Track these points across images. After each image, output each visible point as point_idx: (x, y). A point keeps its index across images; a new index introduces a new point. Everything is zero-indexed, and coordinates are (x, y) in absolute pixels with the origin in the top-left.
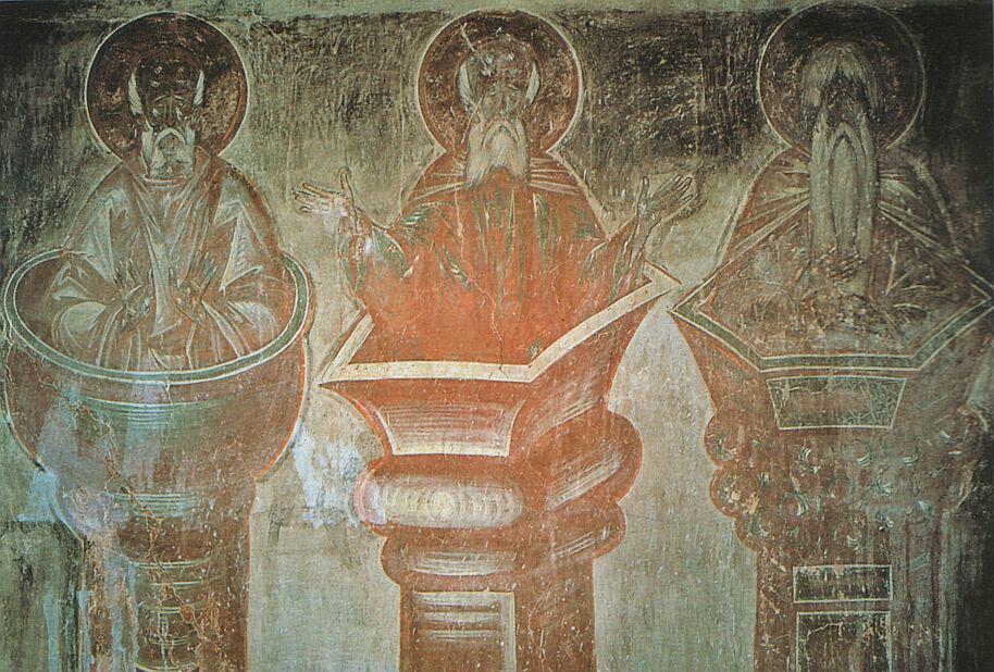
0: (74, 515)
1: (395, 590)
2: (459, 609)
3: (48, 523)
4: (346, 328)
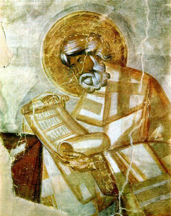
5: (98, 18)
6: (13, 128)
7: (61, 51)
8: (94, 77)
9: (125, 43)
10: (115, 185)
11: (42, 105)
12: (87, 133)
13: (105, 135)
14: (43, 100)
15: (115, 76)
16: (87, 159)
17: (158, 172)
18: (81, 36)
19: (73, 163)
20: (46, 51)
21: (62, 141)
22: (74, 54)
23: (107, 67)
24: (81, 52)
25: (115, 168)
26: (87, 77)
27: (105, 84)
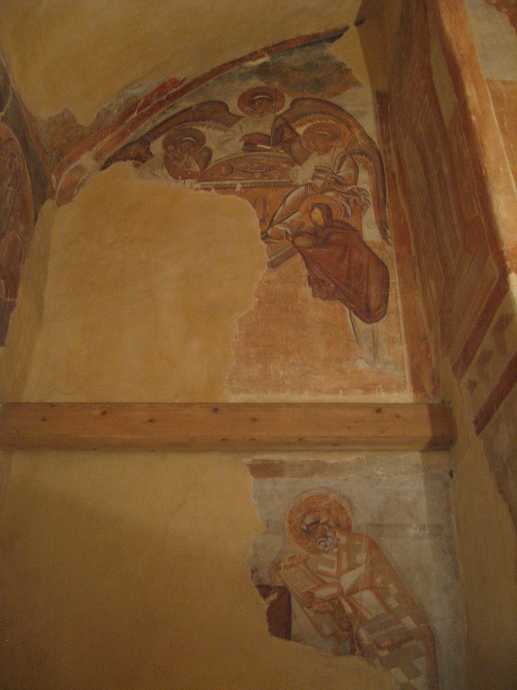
5: (328, 498)
6: (267, 581)
7: (302, 522)
8: (328, 540)
9: (350, 514)
10: (350, 623)
11: (289, 563)
12: (325, 583)
13: (339, 585)
14: (290, 559)
15: (343, 539)
16: (326, 604)
17: (382, 611)
18: (316, 511)
19: (315, 607)
20: (290, 522)
21: (306, 590)
22: (312, 524)
23: (337, 533)
24: (316, 523)
25: (349, 610)
26: (322, 541)
27: (337, 546)
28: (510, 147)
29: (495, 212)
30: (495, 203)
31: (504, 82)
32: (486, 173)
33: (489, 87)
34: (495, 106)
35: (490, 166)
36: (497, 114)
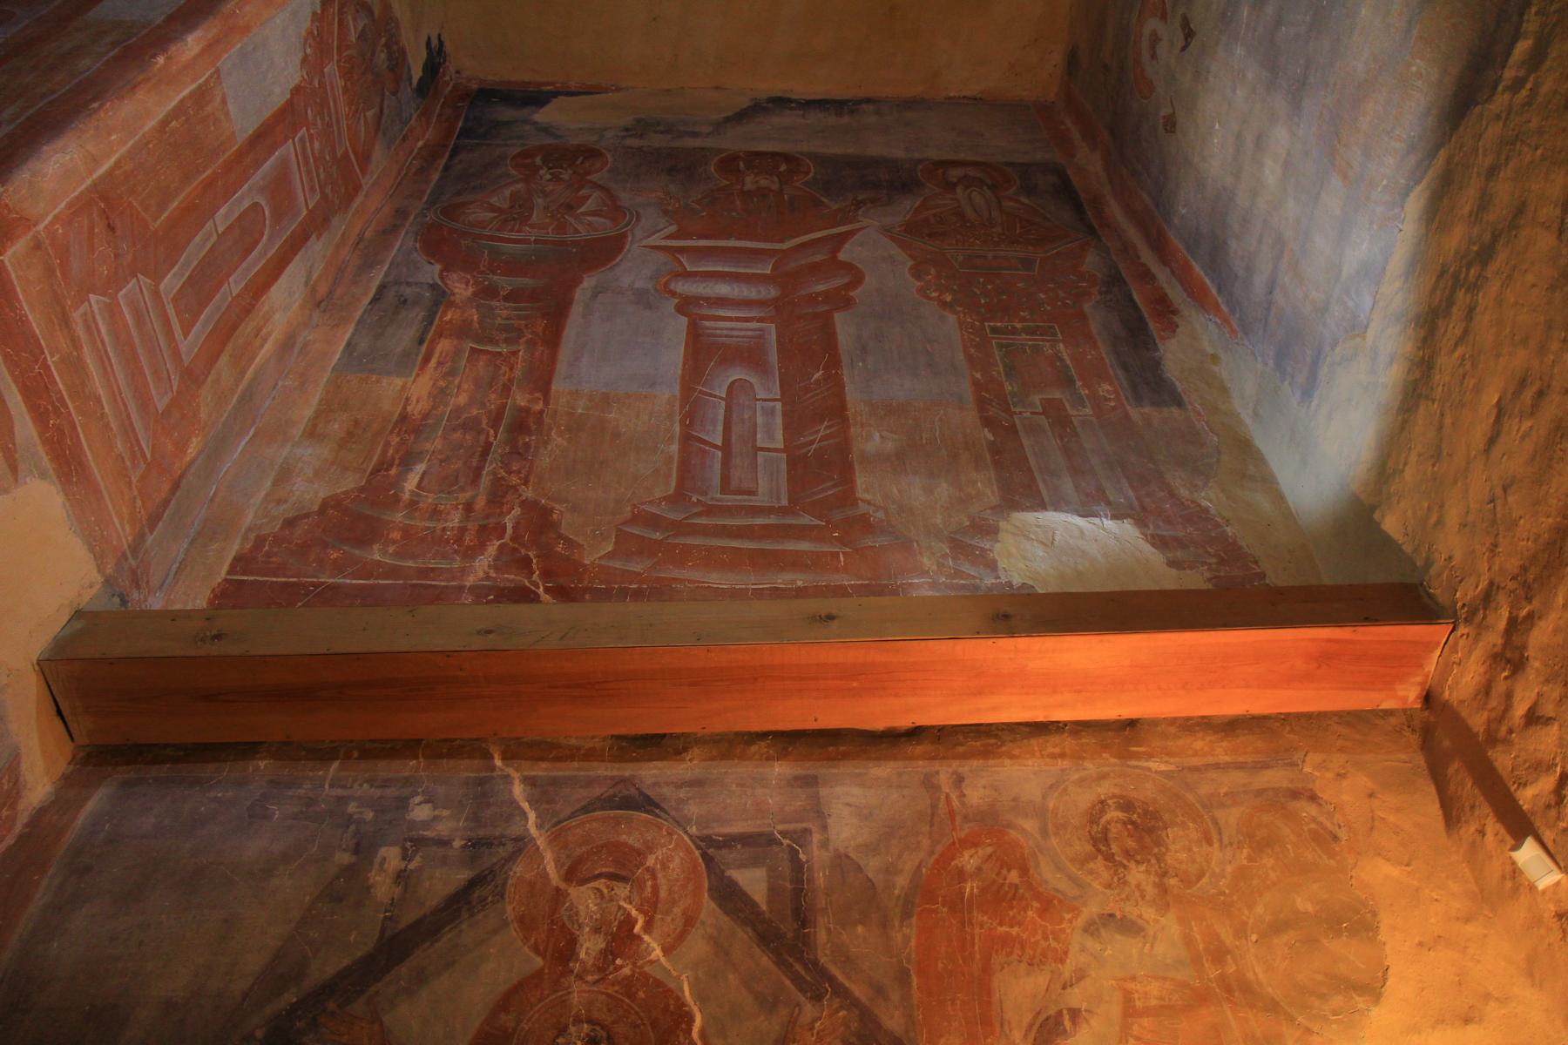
0: (448, 282)
1: (683, 321)
2: (732, 329)
3: (428, 284)
4: (659, 228)
28: (149, 142)
29: (45, 148)
30: (60, 143)
31: (224, 101)
32: (96, 111)
33: (211, 77)
34: (192, 95)
35: (111, 114)
36: (182, 101)
